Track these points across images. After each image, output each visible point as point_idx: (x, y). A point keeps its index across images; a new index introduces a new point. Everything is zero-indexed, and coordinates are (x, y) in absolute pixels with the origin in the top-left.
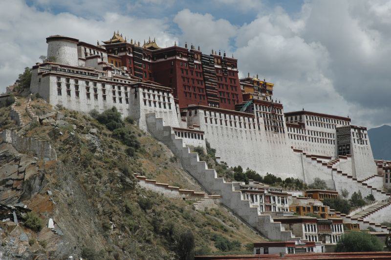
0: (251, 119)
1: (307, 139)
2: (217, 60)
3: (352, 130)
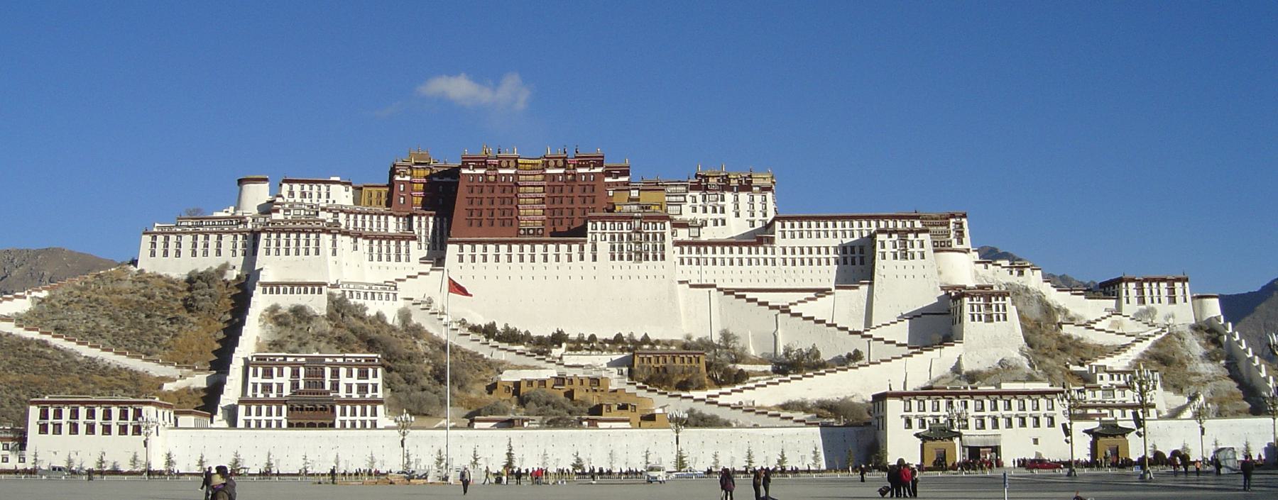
0: (575, 247)
1: (779, 261)
3: (880, 237)
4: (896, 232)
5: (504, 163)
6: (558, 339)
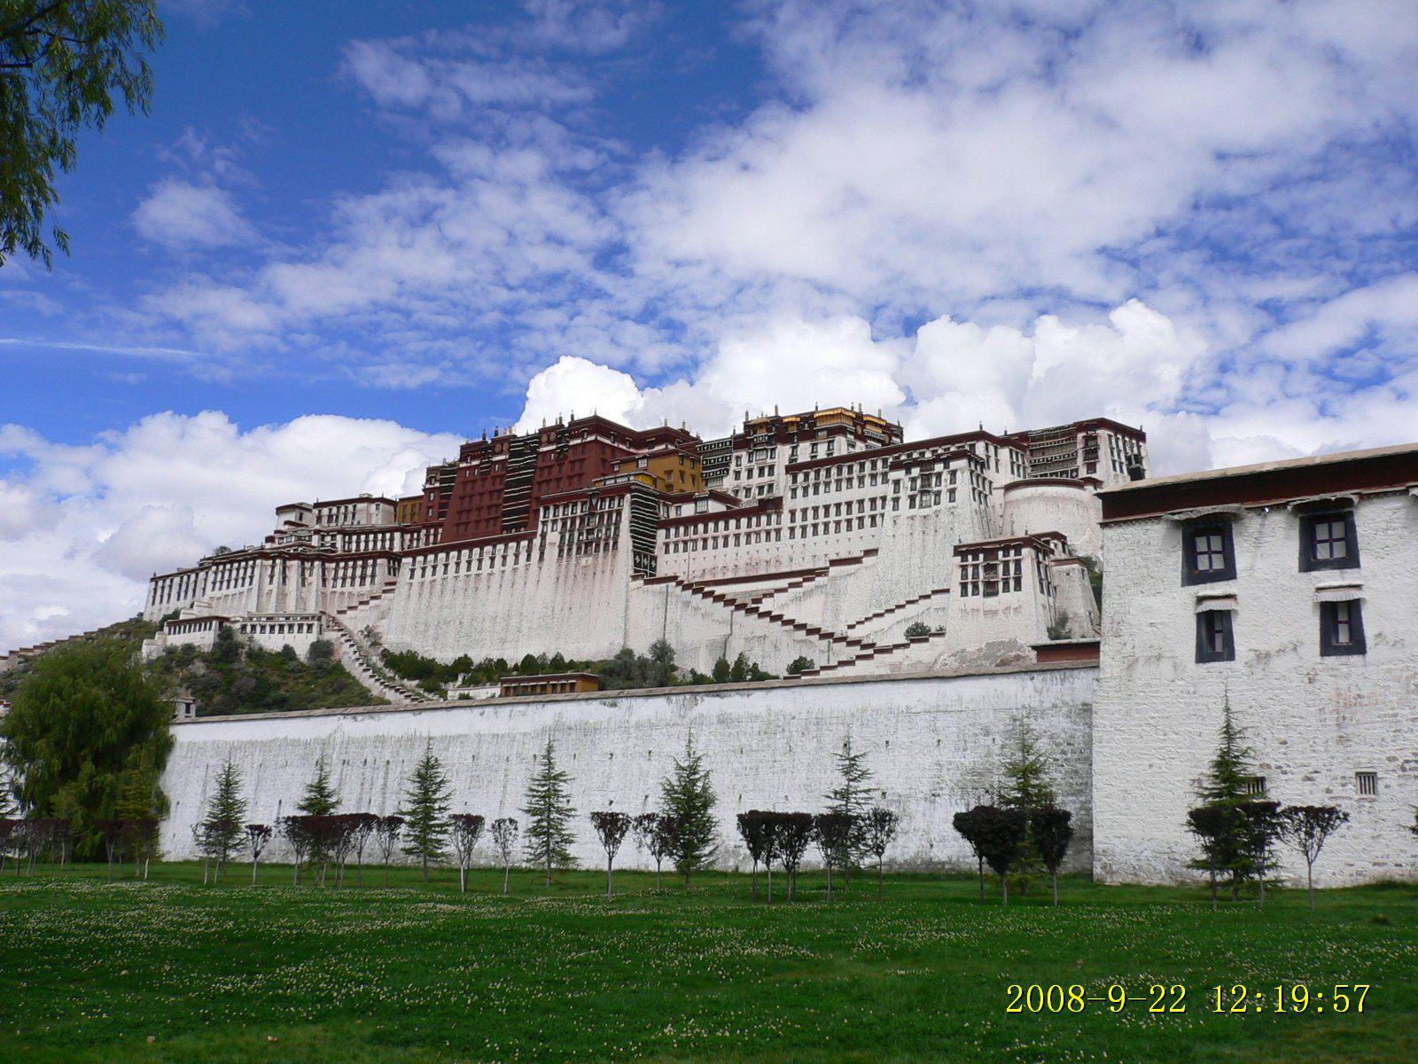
1: (785, 533)
2: (549, 436)
3: (893, 475)
4: (916, 463)
5: (498, 448)
6: (463, 664)
